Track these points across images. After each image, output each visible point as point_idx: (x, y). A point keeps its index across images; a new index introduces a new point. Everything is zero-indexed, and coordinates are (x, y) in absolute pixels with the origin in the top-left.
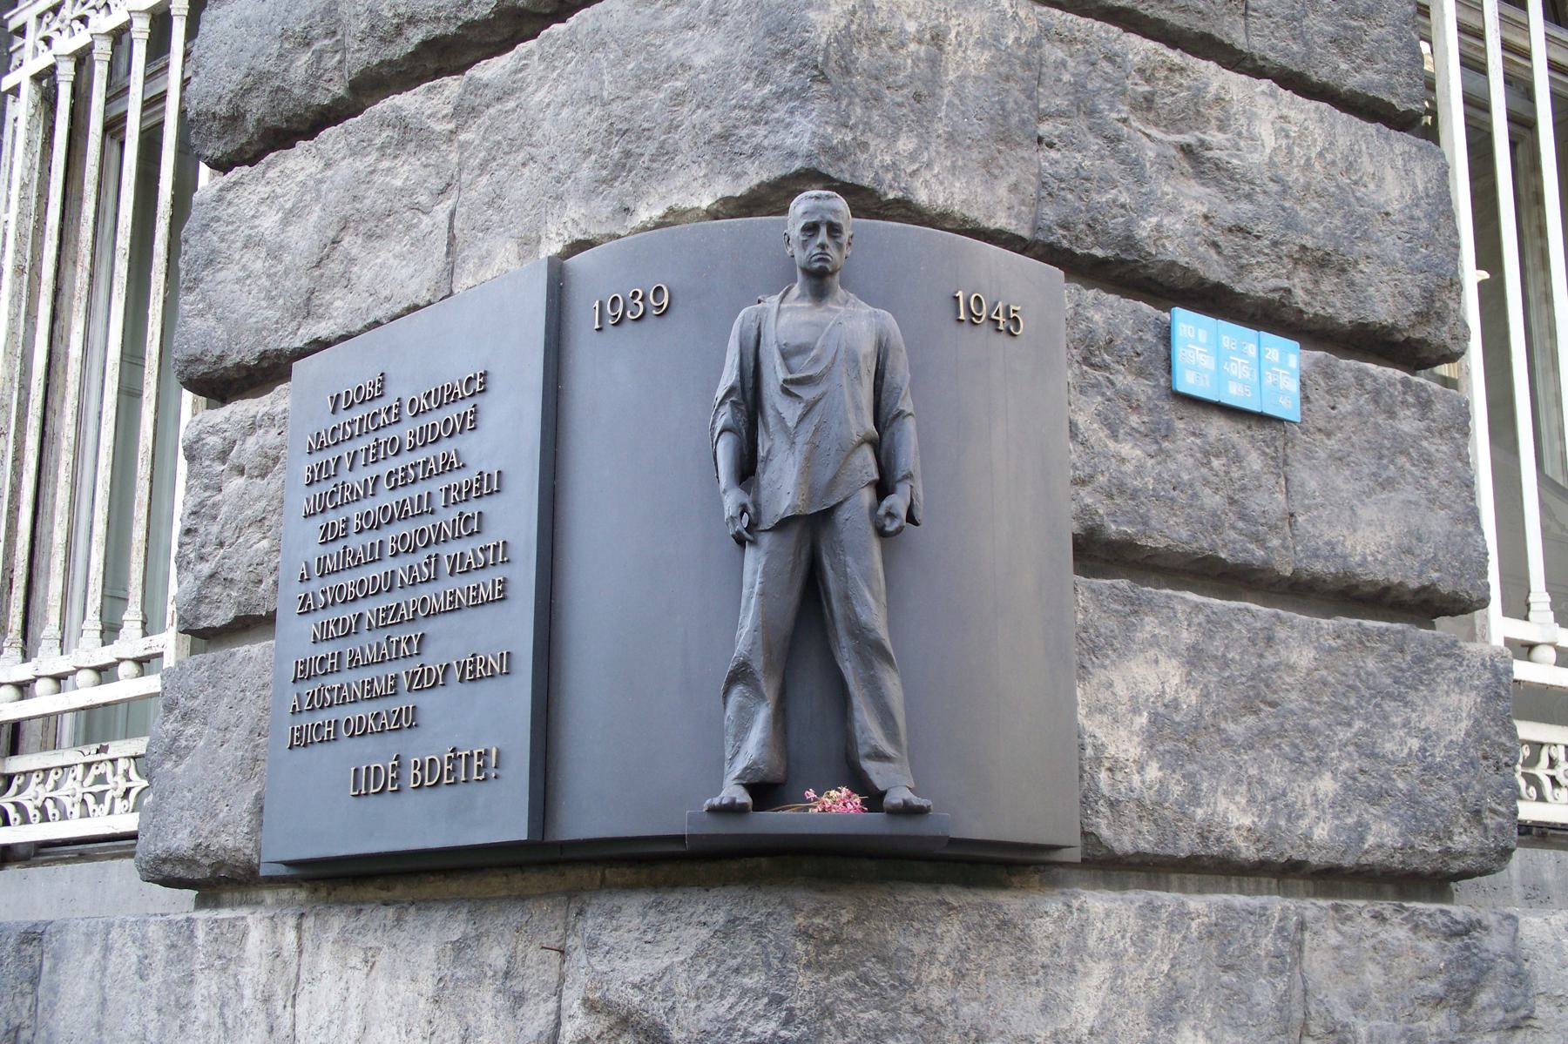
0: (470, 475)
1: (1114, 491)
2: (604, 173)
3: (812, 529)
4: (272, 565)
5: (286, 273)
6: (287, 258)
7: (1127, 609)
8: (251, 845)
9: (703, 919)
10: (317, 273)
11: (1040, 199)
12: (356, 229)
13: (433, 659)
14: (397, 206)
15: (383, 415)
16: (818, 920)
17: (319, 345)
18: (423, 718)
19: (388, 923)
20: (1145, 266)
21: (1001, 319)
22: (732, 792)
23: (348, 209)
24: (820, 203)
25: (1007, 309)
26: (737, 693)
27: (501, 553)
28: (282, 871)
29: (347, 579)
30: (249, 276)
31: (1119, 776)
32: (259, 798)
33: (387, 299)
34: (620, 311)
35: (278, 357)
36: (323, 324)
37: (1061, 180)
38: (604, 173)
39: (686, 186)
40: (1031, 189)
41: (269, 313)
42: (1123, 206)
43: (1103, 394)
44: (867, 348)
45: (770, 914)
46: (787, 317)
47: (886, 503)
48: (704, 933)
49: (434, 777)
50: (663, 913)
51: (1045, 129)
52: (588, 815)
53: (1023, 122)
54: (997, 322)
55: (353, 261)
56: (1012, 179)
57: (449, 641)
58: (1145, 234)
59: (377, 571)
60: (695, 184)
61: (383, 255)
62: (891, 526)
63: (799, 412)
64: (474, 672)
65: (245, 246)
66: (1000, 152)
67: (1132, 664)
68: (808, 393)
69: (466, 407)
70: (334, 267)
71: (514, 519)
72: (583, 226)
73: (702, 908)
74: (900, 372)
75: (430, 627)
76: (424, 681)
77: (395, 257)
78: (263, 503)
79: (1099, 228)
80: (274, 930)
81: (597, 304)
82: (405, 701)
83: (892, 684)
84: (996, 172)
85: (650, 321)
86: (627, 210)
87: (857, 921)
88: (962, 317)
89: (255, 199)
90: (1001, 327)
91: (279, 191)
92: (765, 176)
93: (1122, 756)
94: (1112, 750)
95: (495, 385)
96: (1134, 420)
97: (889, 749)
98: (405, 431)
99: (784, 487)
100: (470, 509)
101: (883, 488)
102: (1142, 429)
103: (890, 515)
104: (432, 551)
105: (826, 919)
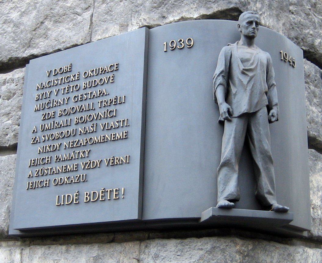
0: (112, 97)
1: (311, 121)
2: (155, 5)
3: (248, 118)
4: (13, 129)
5: (22, 32)
6: (22, 27)
7: (314, 158)
8: (5, 224)
9: (200, 247)
10: (34, 33)
11: (290, 29)
12: (50, 19)
13: (94, 158)
14: (68, 12)
15: (72, 77)
16: (243, 248)
17: (34, 57)
18: (89, 179)
19: (63, 251)
20: (315, 54)
21: (291, 61)
22: (223, 202)
23: (48, 12)
24: (252, 15)
25: (292, 58)
26: (225, 170)
27: (125, 123)
28: (18, 233)
29: (56, 133)
30: (5, 33)
31: (315, 211)
32: (8, 208)
33: (64, 42)
34: (175, 46)
35: (15, 60)
36: (35, 50)
37: (296, 24)
38: (155, 5)
39: (188, 11)
40: (288, 26)
41: (14, 45)
42: (311, 35)
43: (308, 91)
44: (265, 62)
45: (227, 246)
46: (240, 51)
47: (272, 111)
48: (201, 252)
49: (94, 199)
50: (183, 246)
51: (291, 8)
52: (163, 209)
53: (287, 5)
54: (290, 62)
55: (49, 29)
56: (283, 21)
57: (100, 153)
58: (317, 44)
59: (70, 129)
60: (192, 10)
61: (61, 28)
63: (248, 80)
64: (113, 163)
65: (4, 23)
66: (280, 13)
67: (316, 176)
68: (251, 74)
70: (41, 31)
71: (131, 111)
72: (148, 21)
73: (199, 244)
74: (273, 73)
75: (94, 148)
76: (90, 166)
77: (66, 29)
78: (10, 108)
79: (304, 40)
80: (11, 254)
81: (165, 43)
82: (81, 173)
83: (273, 170)
84: (279, 18)
85: (186, 50)
86: (164, 17)
87: (253, 250)
88: (282, 59)
89: (9, 8)
90: (291, 64)
91: (18, 5)
92: (220, 9)
93: (317, 204)
94: (314, 202)
95: (120, 68)
96: (315, 100)
97: (272, 192)
98: (82, 83)
99: (242, 104)
100: (112, 108)
102: (317, 103)
103: (273, 116)
105: (245, 248)
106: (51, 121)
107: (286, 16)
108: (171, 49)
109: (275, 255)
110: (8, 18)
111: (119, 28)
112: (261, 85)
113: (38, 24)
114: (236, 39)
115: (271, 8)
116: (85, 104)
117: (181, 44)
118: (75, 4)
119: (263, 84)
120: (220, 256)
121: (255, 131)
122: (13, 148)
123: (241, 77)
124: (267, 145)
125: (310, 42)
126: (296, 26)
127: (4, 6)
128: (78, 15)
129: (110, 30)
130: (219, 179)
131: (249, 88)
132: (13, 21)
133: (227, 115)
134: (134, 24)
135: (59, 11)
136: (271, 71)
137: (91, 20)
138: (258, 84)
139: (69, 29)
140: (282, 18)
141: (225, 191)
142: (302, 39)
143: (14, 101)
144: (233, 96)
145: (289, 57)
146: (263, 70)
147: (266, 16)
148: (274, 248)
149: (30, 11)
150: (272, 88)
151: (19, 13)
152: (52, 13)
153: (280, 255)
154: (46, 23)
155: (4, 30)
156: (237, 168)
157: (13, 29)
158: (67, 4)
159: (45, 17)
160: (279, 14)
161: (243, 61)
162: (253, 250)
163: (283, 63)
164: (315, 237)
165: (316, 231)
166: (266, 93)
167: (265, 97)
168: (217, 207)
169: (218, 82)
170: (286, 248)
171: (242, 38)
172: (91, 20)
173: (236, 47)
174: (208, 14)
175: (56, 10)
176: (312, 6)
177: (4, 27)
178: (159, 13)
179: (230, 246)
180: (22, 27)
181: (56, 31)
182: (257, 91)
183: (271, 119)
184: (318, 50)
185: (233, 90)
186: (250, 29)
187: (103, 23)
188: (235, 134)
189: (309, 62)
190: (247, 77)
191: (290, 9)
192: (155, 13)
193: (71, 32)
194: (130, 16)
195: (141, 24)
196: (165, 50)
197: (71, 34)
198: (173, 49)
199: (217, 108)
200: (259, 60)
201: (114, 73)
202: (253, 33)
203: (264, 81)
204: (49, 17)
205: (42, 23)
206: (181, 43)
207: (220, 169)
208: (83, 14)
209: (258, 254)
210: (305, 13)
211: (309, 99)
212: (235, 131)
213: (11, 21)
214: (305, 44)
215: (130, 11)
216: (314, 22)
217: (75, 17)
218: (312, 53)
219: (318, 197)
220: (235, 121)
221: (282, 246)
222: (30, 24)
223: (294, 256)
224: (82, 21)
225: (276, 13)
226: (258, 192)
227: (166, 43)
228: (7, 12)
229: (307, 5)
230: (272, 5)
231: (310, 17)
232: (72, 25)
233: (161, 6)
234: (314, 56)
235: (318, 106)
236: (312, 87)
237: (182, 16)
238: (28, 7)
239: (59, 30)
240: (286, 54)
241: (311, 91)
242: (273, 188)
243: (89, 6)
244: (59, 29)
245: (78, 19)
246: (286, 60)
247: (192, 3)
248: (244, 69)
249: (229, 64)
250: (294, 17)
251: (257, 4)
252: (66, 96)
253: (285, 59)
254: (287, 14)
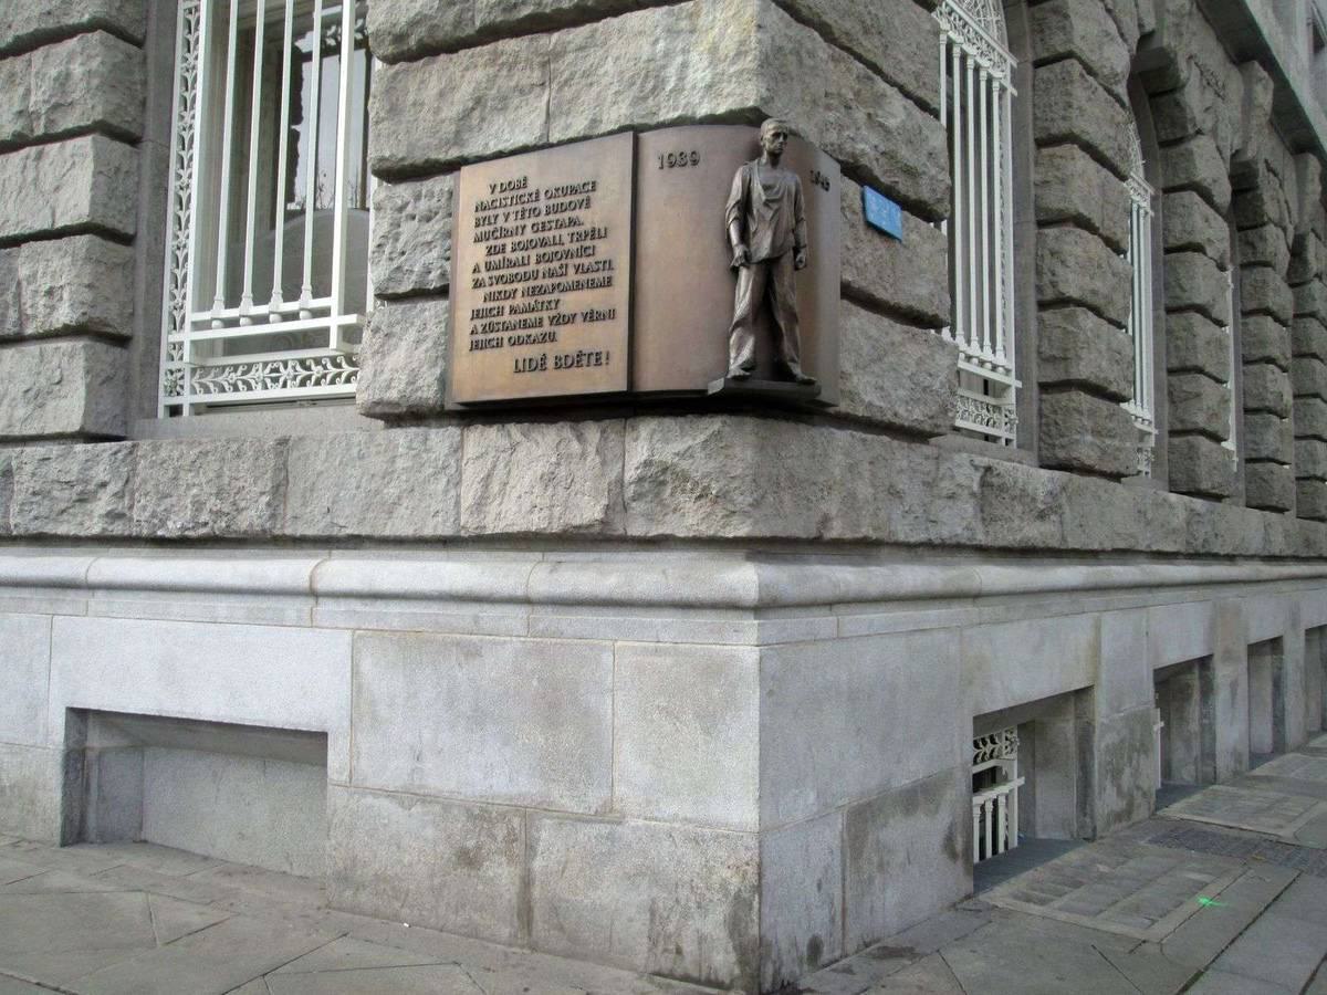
0: (588, 227)
13: (565, 309)
28: (460, 408)
47: (799, 256)
57: (571, 302)
62: (801, 266)
64: (591, 316)
68: (775, 206)
69: (584, 196)
71: (615, 249)
76: (559, 320)
82: (547, 328)
95: (598, 187)
97: (796, 359)
98: (542, 204)
99: (763, 246)
100: (588, 243)
101: (796, 250)
103: (801, 261)
104: (563, 261)
106: (500, 256)
116: (549, 234)
122: (443, 292)
123: (763, 210)
124: (794, 300)
130: (732, 341)
143: (437, 225)
166: (793, 231)
185: (753, 228)
198: (672, 165)
201: (590, 194)
207: (733, 330)
252: (520, 223)
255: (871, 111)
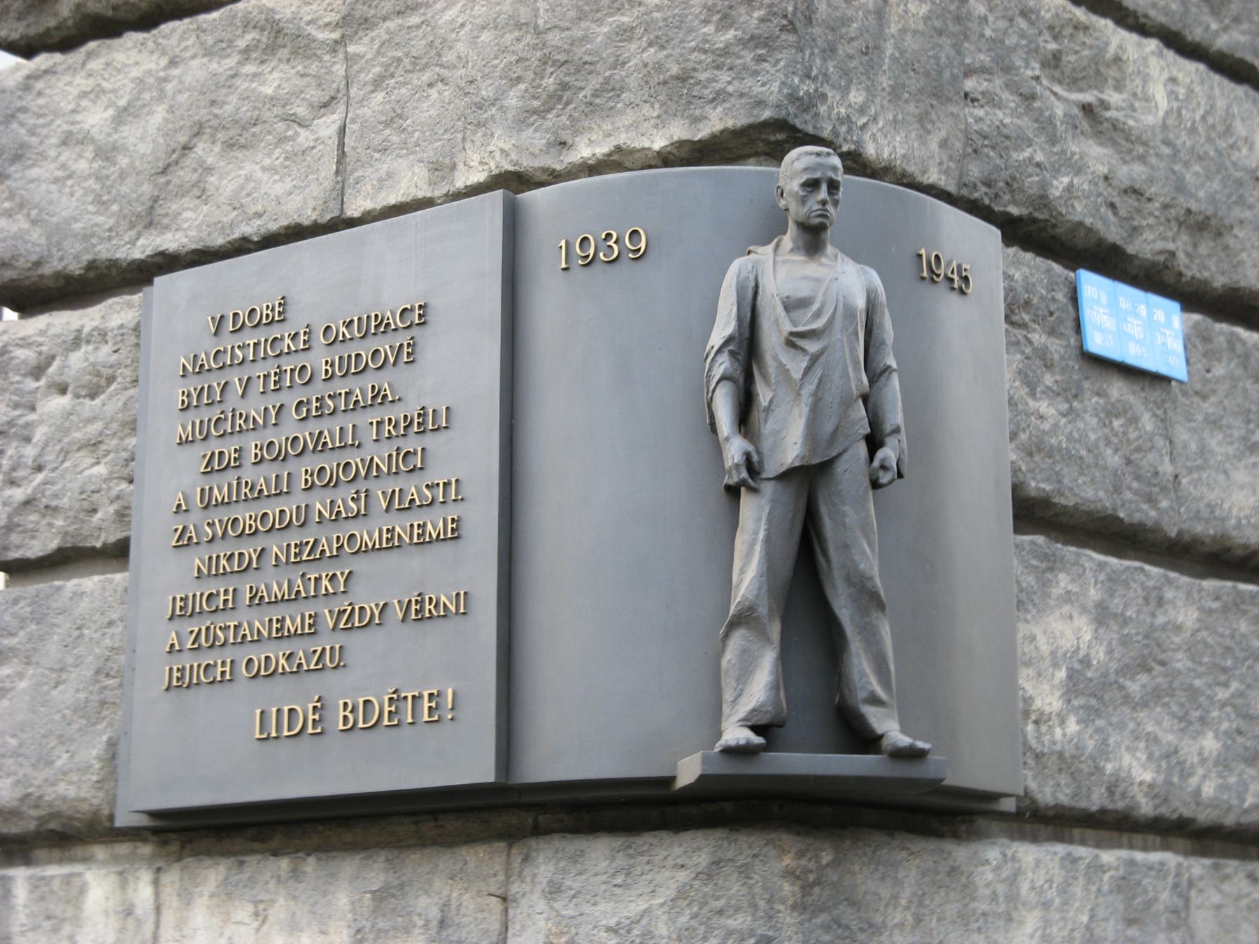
1: (1034, 449)
2: (536, 103)
3: (809, 479)
4: (114, 493)
5: (123, 176)
6: (123, 161)
7: (1044, 565)
8: (101, 794)
9: (680, 861)
10: (162, 180)
11: (965, 156)
12: (212, 136)
14: (266, 115)
15: (287, 341)
16: (803, 862)
18: (349, 658)
19: (283, 874)
20: (1054, 226)
21: (955, 277)
22: (736, 734)
23: (203, 114)
24: (819, 160)
25: (959, 266)
26: (738, 639)
27: (452, 492)
28: (144, 821)
29: (245, 515)
30: (70, 177)
31: (1044, 729)
32: (112, 744)
33: (259, 215)
34: (591, 252)
35: (108, 267)
36: (169, 236)
37: (985, 137)
38: (536, 103)
39: (635, 126)
40: (958, 145)
41: (100, 219)
42: (1038, 165)
43: (1023, 353)
44: (861, 303)
45: (755, 856)
46: (781, 271)
47: (880, 454)
48: (683, 876)
50: (631, 856)
51: (970, 84)
53: (954, 78)
54: (952, 280)
55: (209, 170)
56: (943, 134)
57: (381, 583)
58: (1057, 194)
59: (289, 506)
60: (646, 124)
61: (248, 168)
62: (885, 478)
63: (804, 365)
64: (419, 613)
65: (64, 143)
66: (932, 106)
67: (1051, 619)
68: (812, 347)
69: (403, 338)
70: (185, 174)
71: (470, 456)
72: (513, 156)
73: (678, 851)
74: (888, 328)
75: (361, 565)
76: (354, 622)
77: (264, 169)
78: (98, 426)
79: (1015, 185)
80: (123, 885)
81: (563, 243)
83: (886, 631)
84: (929, 126)
85: (624, 265)
86: (563, 144)
87: (834, 864)
88: (925, 274)
89: (75, 92)
90: (956, 285)
91: (105, 85)
92: (730, 123)
93: (1047, 709)
94: (1038, 703)
96: (1048, 380)
98: (319, 360)
99: (788, 443)
101: (874, 442)
102: (1055, 388)
103: (883, 467)
104: (362, 486)
105: (810, 860)
106: (231, 476)
107: (952, 114)
108: (580, 262)
109: (907, 876)
110: (74, 128)
111: (427, 175)
112: (845, 375)
113: (174, 151)
114: (771, 230)
115: (900, 98)
116: (328, 427)
117: (610, 246)
118: (287, 88)
119: (850, 370)
120: (736, 888)
121: (831, 518)
122: (118, 553)
123: (786, 357)
124: (869, 561)
125: (1031, 192)
126: (986, 142)
127: (60, 84)
128: (300, 125)
129: (399, 183)
130: (724, 663)
131: (809, 388)
132: (93, 141)
133: (744, 474)
134: (472, 164)
135: (238, 109)
136: (881, 326)
137: (341, 144)
138: (836, 378)
139: (272, 170)
140: (938, 124)
141: (744, 699)
142: (1007, 183)
143: (110, 404)
144: (762, 415)
145: (949, 263)
146: (851, 329)
147: (881, 130)
148: (904, 854)
149: (144, 105)
150: (883, 379)
151: (111, 112)
152: (216, 116)
153: (924, 875)
154: (200, 148)
155: (63, 166)
156: (775, 630)
157: (95, 165)
158: (262, 89)
159: (195, 129)
160: (927, 113)
161: (792, 305)
162: (834, 864)
163: (926, 286)
164: (1047, 808)
165: (1048, 790)
166: (865, 398)
167: (860, 411)
168: (716, 750)
169: (718, 372)
170: (943, 851)
171: (792, 229)
172: (341, 144)
173: (771, 261)
174: (696, 139)
175: (229, 108)
176: (1044, 65)
177: (63, 158)
178: (547, 131)
179: (766, 856)
180: (123, 161)
181: (233, 174)
182: (832, 399)
183: (878, 479)
184: (1061, 214)
185: (764, 395)
186: (813, 205)
187: (377, 155)
188: (768, 530)
189: (1029, 256)
190: (801, 357)
191: (967, 89)
192: (535, 131)
193: (281, 180)
194: (460, 136)
195: (493, 165)
196: (564, 265)
197: (279, 189)
198: (590, 263)
199: (718, 450)
200: (841, 297)
201: (415, 332)
202: (820, 216)
203: (856, 363)
204: (208, 130)
205: (187, 148)
206: (611, 243)
207: (727, 635)
208: (316, 122)
209: (854, 874)
210: (1021, 95)
211: (1026, 376)
212: (770, 520)
213: (85, 139)
214: (1018, 197)
215: (459, 119)
216: (1050, 120)
217: (290, 133)
218: (1042, 225)
219: (1053, 686)
220: (768, 488)
221: (932, 844)
222: (149, 151)
223: (972, 873)
224: (314, 147)
225: (917, 111)
226: (842, 697)
227: (567, 242)
228: (70, 107)
229: (1027, 66)
230: (903, 86)
231: (1037, 104)
232: (281, 160)
233: (552, 109)
234: (1049, 230)
235: (1058, 394)
236: (1038, 338)
237: (616, 143)
238: (140, 93)
239: (242, 172)
240: (937, 257)
241: (1035, 350)
242: (886, 683)
243: (333, 98)
244: (240, 168)
245: (300, 140)
246: (938, 276)
247: (645, 102)
248: (792, 334)
249: (749, 315)
250: (981, 113)
251: (852, 95)
252: (272, 402)
253: (933, 272)
254: (954, 109)
255: (1088, 97)
